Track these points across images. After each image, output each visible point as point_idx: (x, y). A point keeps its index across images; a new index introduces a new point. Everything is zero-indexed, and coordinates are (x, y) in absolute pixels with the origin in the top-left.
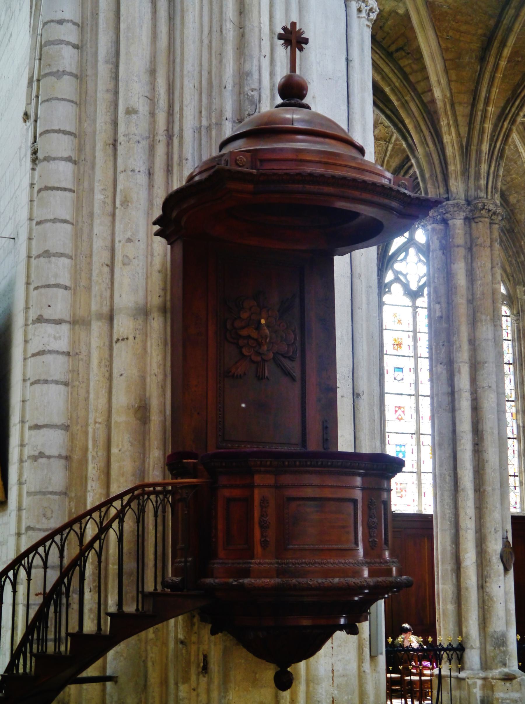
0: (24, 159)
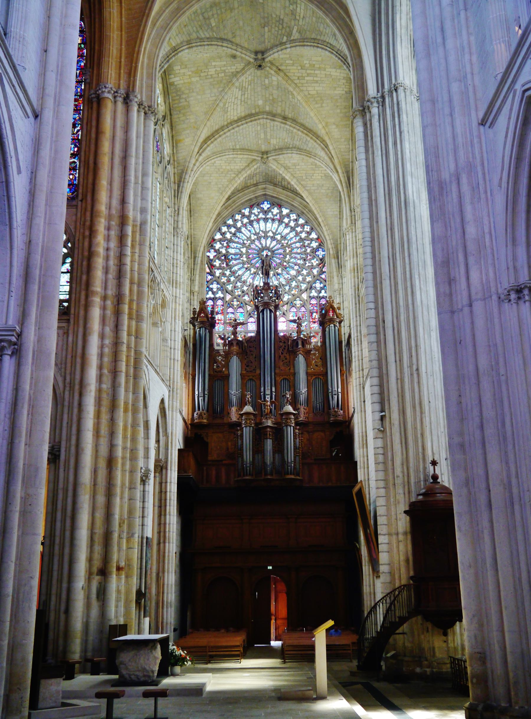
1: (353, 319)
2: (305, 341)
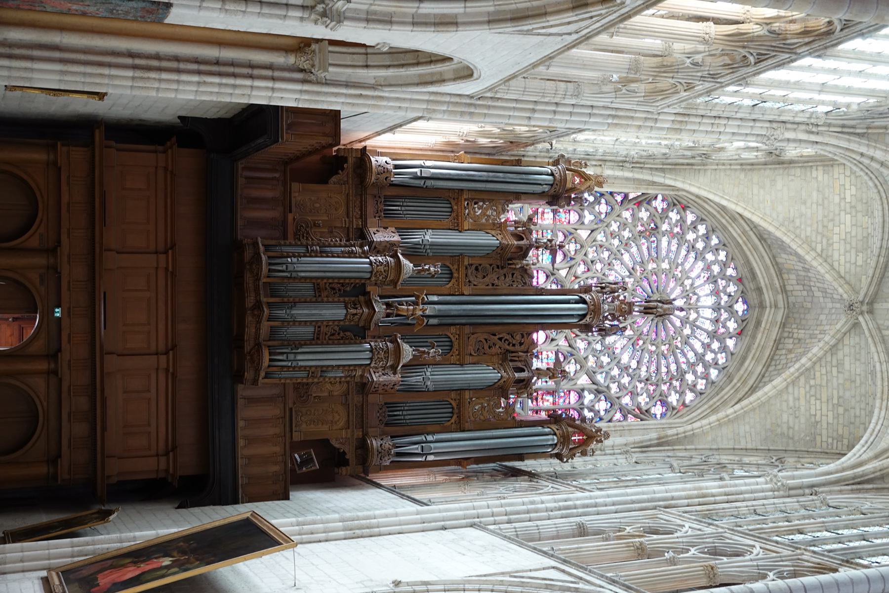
0: (362, 586)
1: (608, 496)
2: (524, 386)
